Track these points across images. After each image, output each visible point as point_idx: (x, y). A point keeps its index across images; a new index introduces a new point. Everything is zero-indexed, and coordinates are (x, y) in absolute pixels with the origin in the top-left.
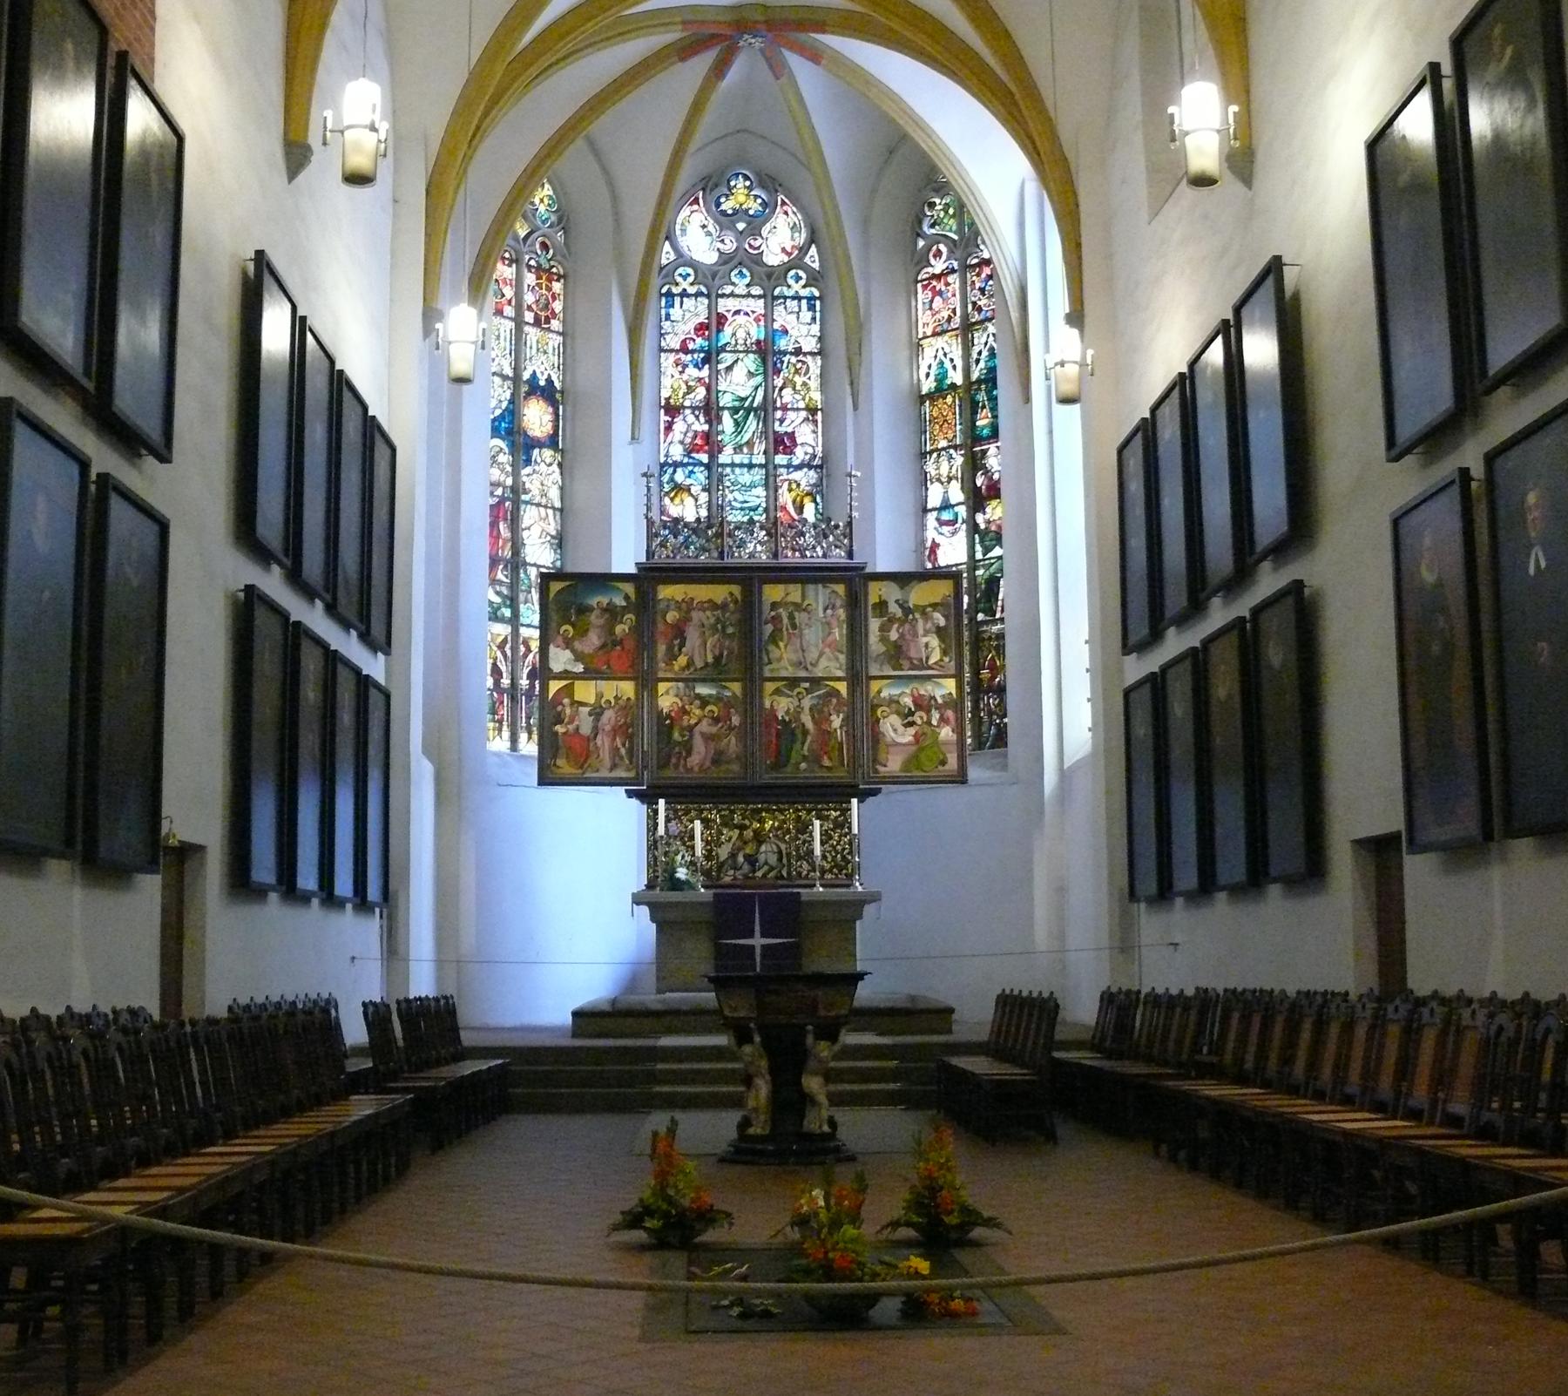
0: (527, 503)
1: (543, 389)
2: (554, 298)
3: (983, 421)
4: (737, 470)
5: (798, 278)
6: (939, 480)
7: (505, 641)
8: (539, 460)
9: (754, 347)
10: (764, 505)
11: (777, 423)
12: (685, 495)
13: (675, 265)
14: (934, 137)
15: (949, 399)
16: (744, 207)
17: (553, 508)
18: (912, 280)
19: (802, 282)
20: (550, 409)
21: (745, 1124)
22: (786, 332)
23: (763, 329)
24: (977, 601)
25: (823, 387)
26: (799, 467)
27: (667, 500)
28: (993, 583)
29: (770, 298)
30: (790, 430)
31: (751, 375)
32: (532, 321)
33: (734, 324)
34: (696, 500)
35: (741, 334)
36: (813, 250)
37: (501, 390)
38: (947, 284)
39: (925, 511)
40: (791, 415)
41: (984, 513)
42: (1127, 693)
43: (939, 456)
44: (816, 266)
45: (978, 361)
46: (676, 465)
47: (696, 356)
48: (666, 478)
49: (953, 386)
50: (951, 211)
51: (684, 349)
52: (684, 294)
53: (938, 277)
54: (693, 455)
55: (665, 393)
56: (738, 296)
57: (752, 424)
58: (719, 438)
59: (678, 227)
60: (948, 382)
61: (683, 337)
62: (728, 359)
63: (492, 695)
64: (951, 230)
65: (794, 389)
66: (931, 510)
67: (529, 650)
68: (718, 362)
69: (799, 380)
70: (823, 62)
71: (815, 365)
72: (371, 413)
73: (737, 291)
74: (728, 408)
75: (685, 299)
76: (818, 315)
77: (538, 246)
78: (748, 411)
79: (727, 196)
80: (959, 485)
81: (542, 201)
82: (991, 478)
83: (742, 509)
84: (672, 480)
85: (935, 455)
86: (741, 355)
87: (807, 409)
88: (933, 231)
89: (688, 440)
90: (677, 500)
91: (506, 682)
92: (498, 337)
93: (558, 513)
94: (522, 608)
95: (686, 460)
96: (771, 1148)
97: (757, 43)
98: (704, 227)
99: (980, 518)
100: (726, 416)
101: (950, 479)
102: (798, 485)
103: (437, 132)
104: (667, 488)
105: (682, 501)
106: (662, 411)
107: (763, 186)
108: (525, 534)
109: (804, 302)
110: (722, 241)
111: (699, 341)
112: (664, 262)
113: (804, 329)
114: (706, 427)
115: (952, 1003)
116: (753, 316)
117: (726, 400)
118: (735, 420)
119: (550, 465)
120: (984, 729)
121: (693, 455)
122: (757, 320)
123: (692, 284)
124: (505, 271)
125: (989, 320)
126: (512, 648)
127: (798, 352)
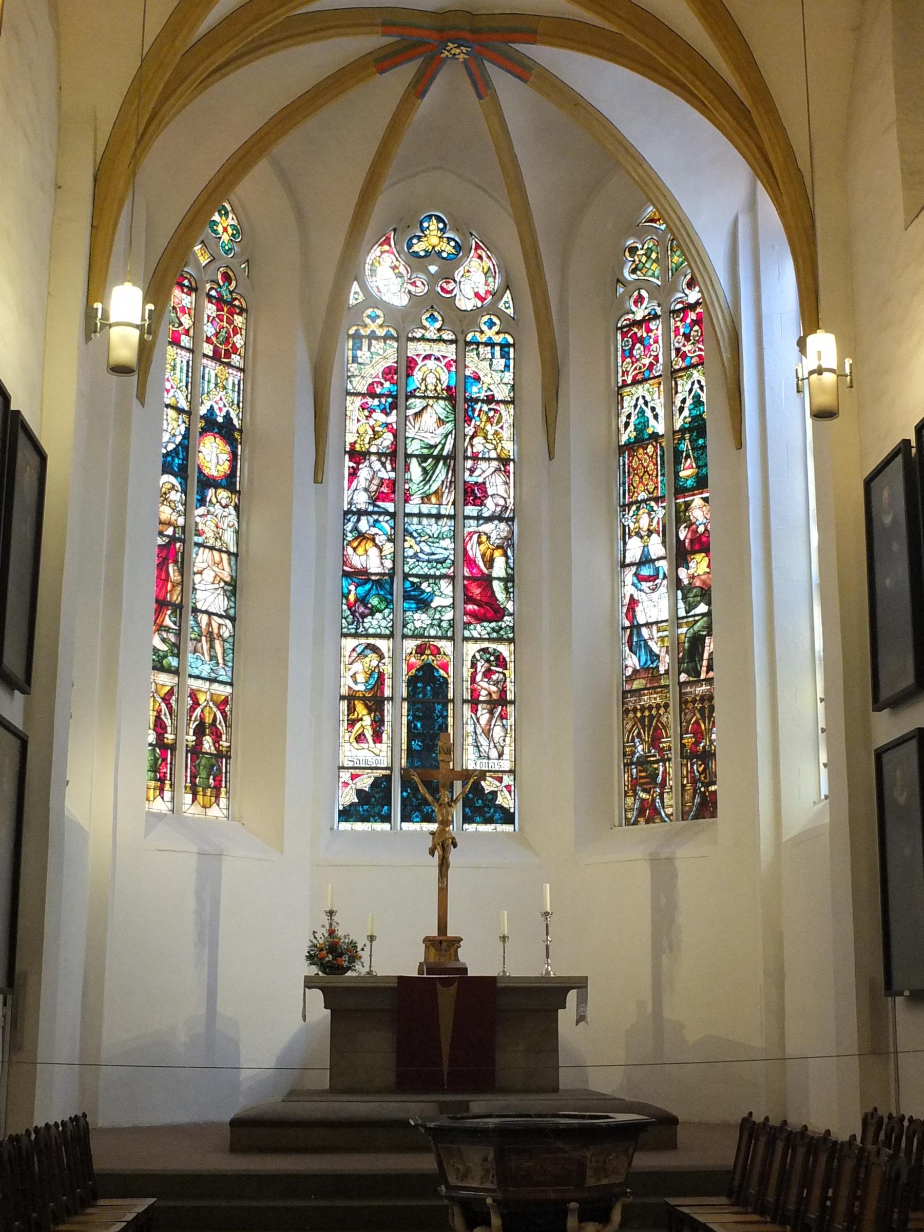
0: (199, 545)
2: (235, 333)
4: (425, 521)
5: (491, 324)
6: (638, 534)
8: (214, 500)
9: (445, 394)
10: (452, 557)
11: (467, 473)
12: (370, 544)
13: (361, 307)
14: (645, 166)
16: (437, 249)
17: (228, 553)
18: (612, 327)
19: (496, 329)
20: (228, 448)
22: (477, 379)
23: (453, 375)
25: (517, 437)
27: (350, 550)
29: (461, 343)
30: (480, 480)
31: (441, 422)
32: (211, 354)
33: (424, 369)
34: (381, 551)
35: (431, 380)
36: (507, 296)
37: (175, 424)
39: (624, 565)
40: (483, 465)
41: (688, 568)
42: (879, 755)
44: (510, 312)
45: (681, 410)
46: (360, 513)
47: (383, 400)
48: (349, 526)
51: (372, 394)
52: (373, 336)
54: (378, 503)
55: (350, 438)
56: (429, 340)
57: (441, 473)
58: (407, 487)
59: (367, 267)
61: (370, 381)
63: (154, 750)
65: (485, 438)
67: (196, 703)
68: (407, 408)
70: (532, 79)
71: (507, 414)
72: (13, 407)
75: (374, 342)
76: (512, 362)
77: (219, 276)
78: (438, 459)
79: (419, 238)
83: (429, 561)
84: (355, 529)
86: (431, 402)
87: (499, 459)
90: (360, 550)
92: (174, 368)
93: (233, 558)
94: (191, 657)
95: (371, 508)
97: (461, 54)
100: (414, 463)
102: (489, 538)
103: (108, 113)
105: (366, 551)
106: (347, 457)
108: (197, 578)
109: (497, 348)
110: (414, 284)
111: (387, 384)
113: (497, 377)
114: (392, 475)
115: (674, 1112)
116: (444, 362)
117: (414, 447)
118: (424, 470)
119: (226, 506)
120: (687, 797)
121: (378, 503)
122: (448, 365)
123: (381, 326)
124: (181, 298)
127: (490, 400)
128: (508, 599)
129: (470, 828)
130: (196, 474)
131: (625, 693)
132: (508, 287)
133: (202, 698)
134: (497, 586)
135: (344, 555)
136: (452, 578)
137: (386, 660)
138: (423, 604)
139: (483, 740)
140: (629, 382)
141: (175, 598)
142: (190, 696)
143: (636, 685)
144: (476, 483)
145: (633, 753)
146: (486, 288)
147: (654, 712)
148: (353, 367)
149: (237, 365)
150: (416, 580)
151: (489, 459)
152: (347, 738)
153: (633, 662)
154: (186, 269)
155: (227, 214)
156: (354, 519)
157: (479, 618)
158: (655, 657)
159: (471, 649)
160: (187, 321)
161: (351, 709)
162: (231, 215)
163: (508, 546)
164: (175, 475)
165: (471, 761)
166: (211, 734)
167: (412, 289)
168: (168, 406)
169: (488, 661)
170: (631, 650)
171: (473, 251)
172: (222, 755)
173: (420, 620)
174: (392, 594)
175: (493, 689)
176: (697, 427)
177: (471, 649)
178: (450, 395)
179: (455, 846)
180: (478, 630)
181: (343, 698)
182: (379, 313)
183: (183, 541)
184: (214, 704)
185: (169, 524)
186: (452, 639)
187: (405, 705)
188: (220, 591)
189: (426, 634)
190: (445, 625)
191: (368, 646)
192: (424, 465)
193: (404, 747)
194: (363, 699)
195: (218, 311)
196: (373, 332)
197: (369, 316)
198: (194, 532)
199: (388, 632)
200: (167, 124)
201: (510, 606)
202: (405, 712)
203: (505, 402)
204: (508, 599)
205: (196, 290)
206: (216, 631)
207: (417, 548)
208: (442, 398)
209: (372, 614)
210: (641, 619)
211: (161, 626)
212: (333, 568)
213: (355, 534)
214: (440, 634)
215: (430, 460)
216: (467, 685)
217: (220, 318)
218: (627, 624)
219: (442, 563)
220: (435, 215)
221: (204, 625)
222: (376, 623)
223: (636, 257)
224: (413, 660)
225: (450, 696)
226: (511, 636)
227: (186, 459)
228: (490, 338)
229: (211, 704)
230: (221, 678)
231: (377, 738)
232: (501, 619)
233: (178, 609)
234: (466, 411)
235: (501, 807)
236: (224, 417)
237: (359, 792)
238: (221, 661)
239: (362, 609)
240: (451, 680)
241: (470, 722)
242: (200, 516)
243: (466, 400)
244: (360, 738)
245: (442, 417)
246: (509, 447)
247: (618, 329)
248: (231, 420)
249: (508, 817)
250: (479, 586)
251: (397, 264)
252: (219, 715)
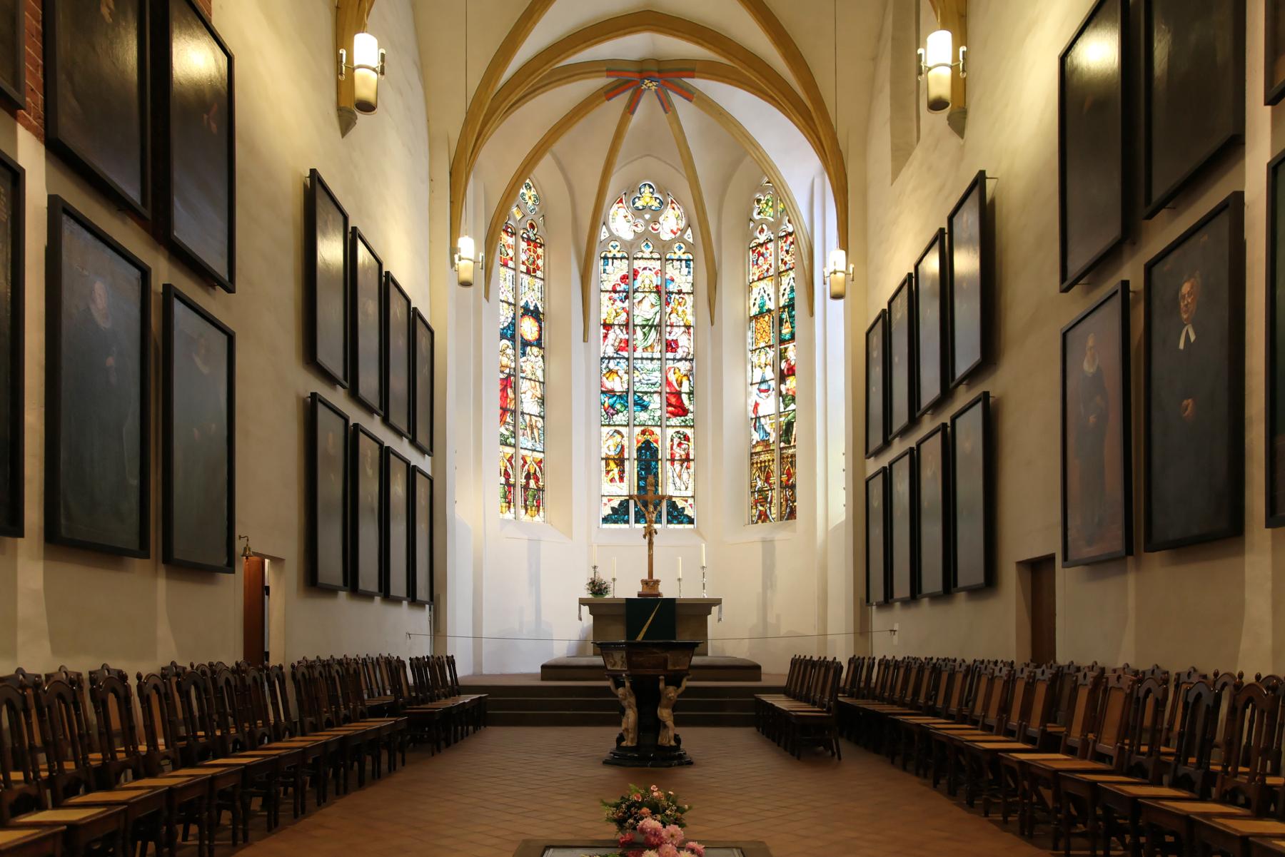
1: (532, 312)
2: (538, 257)
3: (786, 331)
4: (644, 361)
5: (680, 248)
6: (759, 366)
7: (512, 457)
8: (530, 353)
9: (655, 290)
10: (660, 382)
11: (668, 334)
12: (615, 375)
15: (767, 318)
16: (649, 204)
17: (539, 382)
18: (747, 248)
19: (683, 250)
20: (537, 324)
21: (621, 739)
23: (659, 278)
24: (781, 436)
25: (695, 313)
26: (680, 360)
27: (604, 379)
28: (790, 425)
29: (663, 260)
30: (675, 338)
31: (653, 306)
32: (525, 271)
34: (621, 379)
35: (647, 282)
36: (689, 231)
37: (507, 312)
38: (767, 249)
40: (675, 329)
43: (760, 352)
44: (691, 240)
45: (784, 294)
46: (610, 358)
47: (621, 294)
49: (769, 311)
50: (770, 204)
51: (615, 291)
52: (614, 258)
53: (761, 245)
54: (619, 352)
56: (645, 259)
58: (635, 343)
59: (610, 217)
60: (766, 308)
62: (639, 296)
64: (770, 216)
65: (677, 314)
66: (755, 384)
67: (525, 462)
68: (634, 298)
69: (680, 309)
71: (689, 300)
73: (645, 256)
74: (640, 326)
75: (615, 260)
76: (692, 270)
77: (528, 225)
78: (651, 326)
80: (771, 368)
81: (530, 198)
82: (790, 364)
83: (647, 384)
84: (607, 367)
85: (758, 351)
86: (647, 294)
88: (759, 217)
89: (616, 344)
90: (610, 379)
91: (512, 480)
93: (542, 385)
94: (521, 438)
95: (615, 356)
96: (636, 755)
98: (625, 217)
99: (783, 387)
100: (638, 329)
101: (766, 365)
102: (680, 370)
104: (604, 372)
105: (613, 379)
107: (660, 192)
108: (523, 396)
109: (684, 262)
110: (636, 226)
112: (603, 238)
113: (684, 278)
114: (627, 337)
116: (654, 271)
117: (638, 321)
118: (644, 333)
119: (537, 356)
122: (656, 273)
124: (506, 239)
125: (791, 269)
126: (515, 461)
127: (680, 292)
128: (691, 404)
129: (671, 526)
130: (520, 339)
131: (752, 454)
132: (689, 226)
133: (528, 460)
134: (685, 398)
135: (601, 382)
136: (660, 393)
137: (625, 438)
138: (645, 408)
139: (677, 480)
140: (756, 280)
141: (512, 406)
142: (522, 458)
143: (758, 449)
144: (672, 340)
145: (756, 486)
146: (677, 226)
147: (767, 464)
148: (604, 276)
149: (540, 276)
150: (640, 395)
151: (679, 326)
152: (605, 480)
153: (756, 437)
154: (509, 222)
155: (530, 188)
156: (607, 361)
157: (675, 415)
158: (768, 434)
159: (670, 432)
160: (511, 253)
161: (607, 465)
162: (533, 189)
163: (690, 374)
164: (509, 340)
165: (670, 491)
166: (534, 478)
167: (636, 229)
168: (503, 301)
169: (680, 438)
170: (755, 430)
171: (669, 205)
172: (540, 489)
173: (643, 416)
174: (628, 403)
175: (683, 453)
176: (791, 306)
177: (670, 432)
178: (658, 291)
179: (656, 533)
180: (675, 421)
181: (602, 459)
182: (617, 243)
183: (515, 376)
184: (535, 463)
185: (507, 367)
186: (660, 426)
187: (636, 462)
188: (536, 403)
189: (646, 424)
190: (656, 419)
191: (616, 431)
192: (644, 330)
193: (636, 484)
194: (614, 459)
195: (528, 245)
196: (614, 255)
197: (612, 246)
198: (520, 371)
199: (626, 424)
200: (488, 139)
201: (691, 408)
202: (636, 466)
203: (688, 293)
204: (691, 404)
205: (515, 234)
206: (534, 424)
207: (641, 377)
208: (653, 292)
209: (617, 413)
210: (761, 413)
211: (505, 422)
212: (596, 390)
213: (607, 370)
214: (653, 424)
215: (647, 328)
216: (669, 451)
217: (529, 250)
218: (754, 416)
219: (654, 385)
220: (649, 184)
221: (528, 421)
222: (619, 419)
223: (761, 205)
224: (640, 438)
225: (660, 457)
226: (692, 424)
227: (514, 330)
228: (679, 257)
229: (533, 463)
230: (537, 449)
231: (621, 479)
232: (686, 415)
233: (514, 412)
234: (666, 299)
235: (687, 516)
236: (534, 306)
237: (613, 509)
238: (537, 440)
239: (612, 411)
240: (660, 449)
241: (670, 471)
242: (524, 362)
243: (667, 293)
244: (612, 480)
245: (654, 303)
246: (691, 320)
247: (750, 248)
248: (538, 308)
249: (691, 521)
250: (675, 397)
251: (627, 214)
252: (538, 469)
